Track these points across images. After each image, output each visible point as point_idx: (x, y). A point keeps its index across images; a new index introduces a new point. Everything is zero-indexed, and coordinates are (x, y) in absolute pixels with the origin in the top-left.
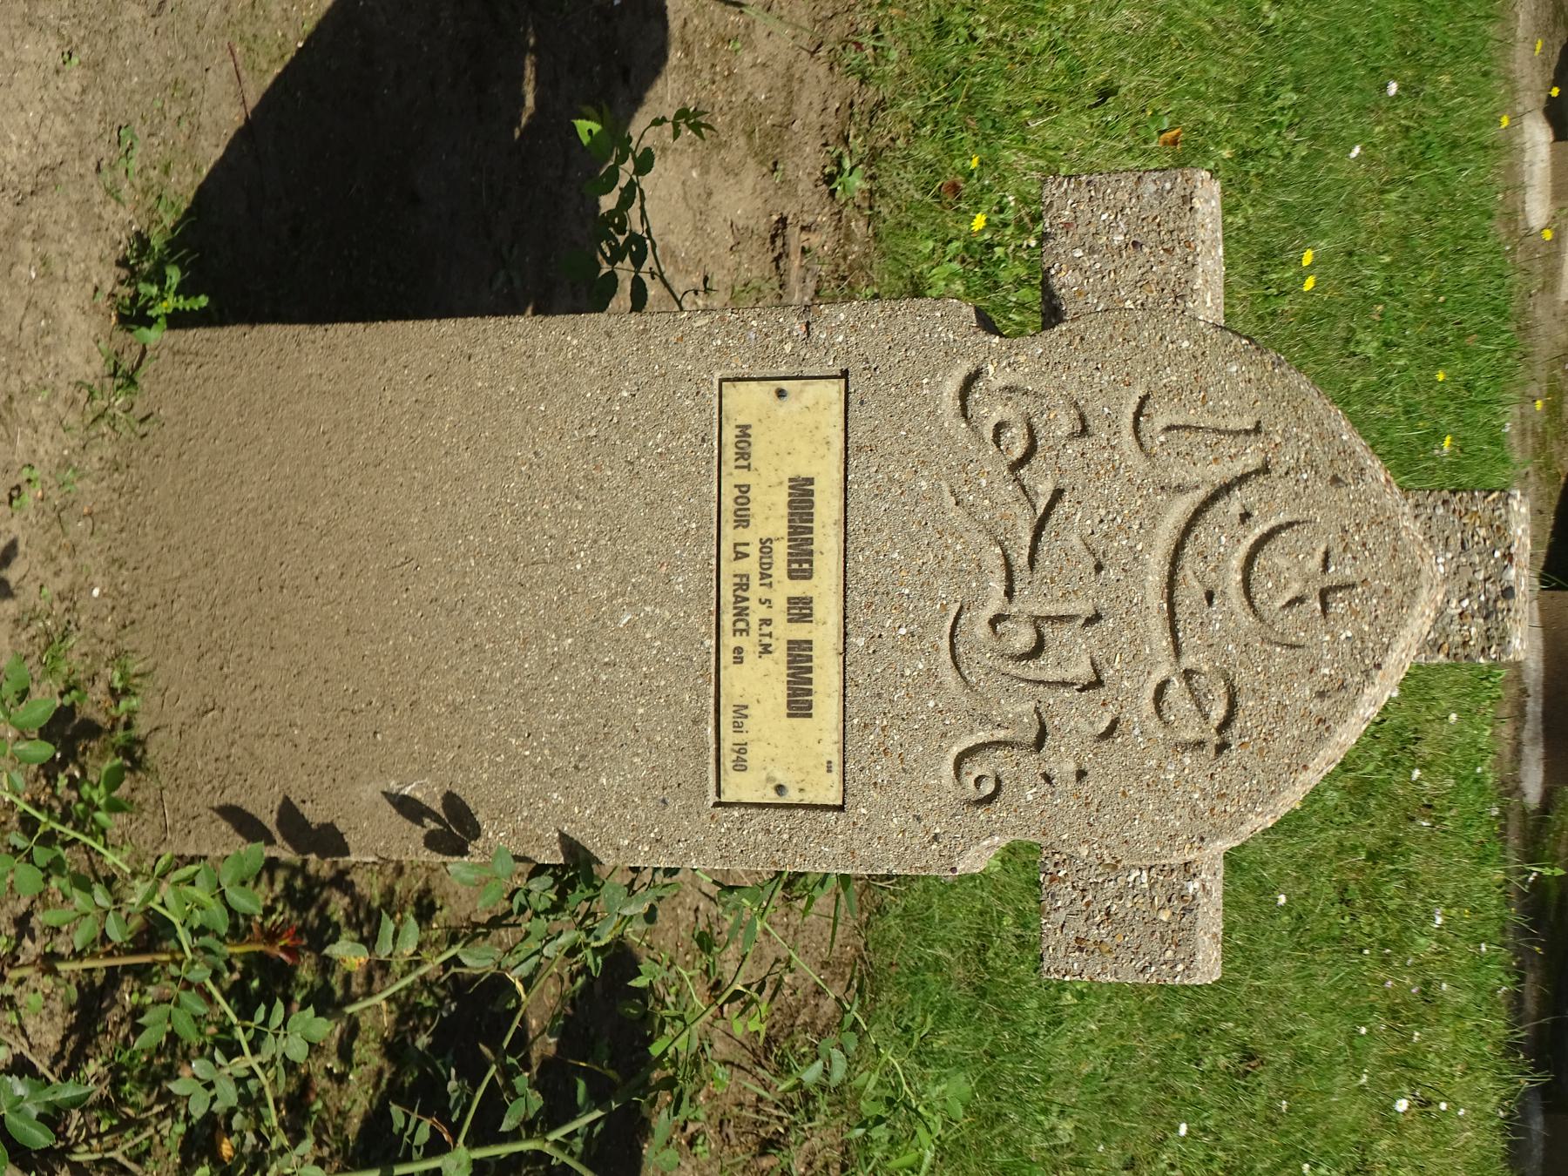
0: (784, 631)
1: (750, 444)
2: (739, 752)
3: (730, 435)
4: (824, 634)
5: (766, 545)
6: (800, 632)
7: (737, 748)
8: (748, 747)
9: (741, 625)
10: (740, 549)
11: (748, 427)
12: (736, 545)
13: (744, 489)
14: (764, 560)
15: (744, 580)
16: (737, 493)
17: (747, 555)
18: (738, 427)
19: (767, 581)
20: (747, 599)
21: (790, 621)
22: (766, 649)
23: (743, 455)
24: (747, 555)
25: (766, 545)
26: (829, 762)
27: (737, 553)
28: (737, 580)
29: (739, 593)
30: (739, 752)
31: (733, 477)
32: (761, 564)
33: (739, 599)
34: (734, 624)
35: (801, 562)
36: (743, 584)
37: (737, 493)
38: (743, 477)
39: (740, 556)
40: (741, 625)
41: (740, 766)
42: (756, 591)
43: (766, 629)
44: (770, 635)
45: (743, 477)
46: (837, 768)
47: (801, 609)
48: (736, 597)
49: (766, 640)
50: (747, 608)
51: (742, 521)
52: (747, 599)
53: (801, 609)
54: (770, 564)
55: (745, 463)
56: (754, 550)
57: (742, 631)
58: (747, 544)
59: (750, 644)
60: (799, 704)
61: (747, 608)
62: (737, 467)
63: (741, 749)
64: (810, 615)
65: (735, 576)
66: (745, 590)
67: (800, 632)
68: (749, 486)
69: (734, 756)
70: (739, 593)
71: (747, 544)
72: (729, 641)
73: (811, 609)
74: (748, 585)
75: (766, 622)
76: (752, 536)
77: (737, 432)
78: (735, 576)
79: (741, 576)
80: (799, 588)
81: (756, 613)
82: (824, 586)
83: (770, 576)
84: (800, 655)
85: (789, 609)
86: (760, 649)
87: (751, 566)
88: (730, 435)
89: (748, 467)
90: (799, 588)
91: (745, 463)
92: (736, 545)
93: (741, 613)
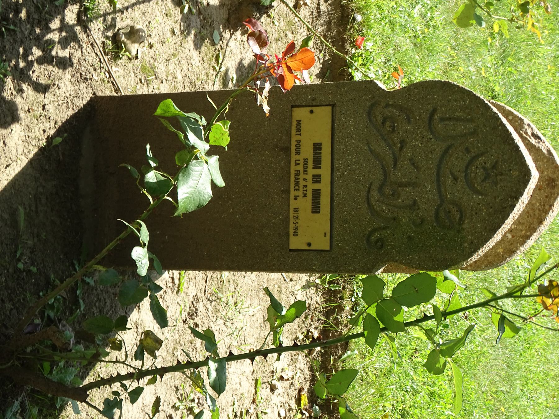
0: (311, 186)
1: (301, 127)
2: (295, 230)
3: (294, 123)
4: (325, 187)
5: (306, 161)
6: (316, 186)
7: (294, 228)
8: (298, 228)
9: (297, 187)
10: (297, 162)
11: (300, 121)
12: (296, 160)
13: (299, 142)
14: (305, 166)
15: (298, 172)
16: (296, 143)
17: (299, 164)
18: (297, 121)
19: (306, 173)
20: (299, 179)
21: (313, 183)
22: (305, 195)
23: (299, 130)
24: (299, 164)
25: (306, 161)
26: (325, 233)
27: (295, 163)
28: (296, 172)
29: (297, 177)
30: (295, 230)
31: (294, 139)
32: (304, 167)
33: (296, 179)
34: (295, 187)
35: (317, 164)
36: (297, 174)
37: (296, 143)
38: (298, 138)
39: (297, 164)
40: (297, 187)
41: (296, 234)
42: (302, 176)
43: (305, 189)
44: (306, 191)
45: (298, 138)
46: (328, 235)
47: (317, 179)
48: (295, 178)
49: (305, 192)
50: (299, 182)
51: (298, 153)
52: (299, 179)
53: (317, 179)
54: (307, 167)
55: (299, 133)
56: (302, 162)
57: (297, 190)
58: (299, 160)
59: (300, 193)
60: (316, 208)
61: (299, 182)
62: (296, 134)
63: (296, 229)
64: (320, 181)
65: (295, 171)
66: (299, 176)
67: (316, 186)
68: (300, 141)
69: (294, 231)
70: (297, 177)
71: (299, 160)
72: (293, 193)
73: (320, 178)
74: (299, 174)
75: (306, 186)
76: (301, 157)
77: (296, 123)
78: (295, 171)
79: (297, 171)
80: (317, 172)
81: (302, 183)
82: (325, 171)
83: (307, 171)
84: (316, 194)
85: (313, 179)
86: (303, 195)
87: (300, 168)
88: (294, 123)
89: (300, 135)
90: (317, 172)
91: (299, 133)
92: (296, 160)
93: (297, 183)
